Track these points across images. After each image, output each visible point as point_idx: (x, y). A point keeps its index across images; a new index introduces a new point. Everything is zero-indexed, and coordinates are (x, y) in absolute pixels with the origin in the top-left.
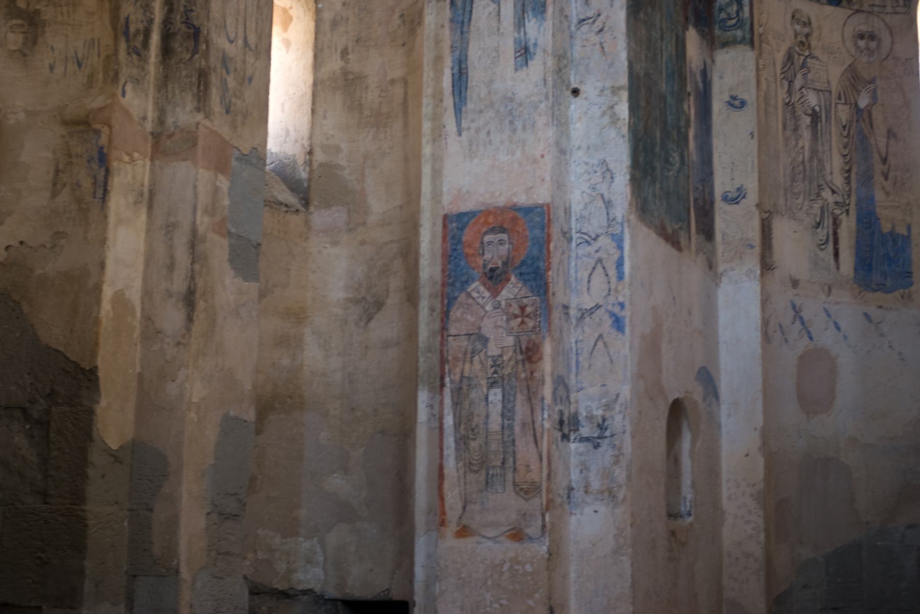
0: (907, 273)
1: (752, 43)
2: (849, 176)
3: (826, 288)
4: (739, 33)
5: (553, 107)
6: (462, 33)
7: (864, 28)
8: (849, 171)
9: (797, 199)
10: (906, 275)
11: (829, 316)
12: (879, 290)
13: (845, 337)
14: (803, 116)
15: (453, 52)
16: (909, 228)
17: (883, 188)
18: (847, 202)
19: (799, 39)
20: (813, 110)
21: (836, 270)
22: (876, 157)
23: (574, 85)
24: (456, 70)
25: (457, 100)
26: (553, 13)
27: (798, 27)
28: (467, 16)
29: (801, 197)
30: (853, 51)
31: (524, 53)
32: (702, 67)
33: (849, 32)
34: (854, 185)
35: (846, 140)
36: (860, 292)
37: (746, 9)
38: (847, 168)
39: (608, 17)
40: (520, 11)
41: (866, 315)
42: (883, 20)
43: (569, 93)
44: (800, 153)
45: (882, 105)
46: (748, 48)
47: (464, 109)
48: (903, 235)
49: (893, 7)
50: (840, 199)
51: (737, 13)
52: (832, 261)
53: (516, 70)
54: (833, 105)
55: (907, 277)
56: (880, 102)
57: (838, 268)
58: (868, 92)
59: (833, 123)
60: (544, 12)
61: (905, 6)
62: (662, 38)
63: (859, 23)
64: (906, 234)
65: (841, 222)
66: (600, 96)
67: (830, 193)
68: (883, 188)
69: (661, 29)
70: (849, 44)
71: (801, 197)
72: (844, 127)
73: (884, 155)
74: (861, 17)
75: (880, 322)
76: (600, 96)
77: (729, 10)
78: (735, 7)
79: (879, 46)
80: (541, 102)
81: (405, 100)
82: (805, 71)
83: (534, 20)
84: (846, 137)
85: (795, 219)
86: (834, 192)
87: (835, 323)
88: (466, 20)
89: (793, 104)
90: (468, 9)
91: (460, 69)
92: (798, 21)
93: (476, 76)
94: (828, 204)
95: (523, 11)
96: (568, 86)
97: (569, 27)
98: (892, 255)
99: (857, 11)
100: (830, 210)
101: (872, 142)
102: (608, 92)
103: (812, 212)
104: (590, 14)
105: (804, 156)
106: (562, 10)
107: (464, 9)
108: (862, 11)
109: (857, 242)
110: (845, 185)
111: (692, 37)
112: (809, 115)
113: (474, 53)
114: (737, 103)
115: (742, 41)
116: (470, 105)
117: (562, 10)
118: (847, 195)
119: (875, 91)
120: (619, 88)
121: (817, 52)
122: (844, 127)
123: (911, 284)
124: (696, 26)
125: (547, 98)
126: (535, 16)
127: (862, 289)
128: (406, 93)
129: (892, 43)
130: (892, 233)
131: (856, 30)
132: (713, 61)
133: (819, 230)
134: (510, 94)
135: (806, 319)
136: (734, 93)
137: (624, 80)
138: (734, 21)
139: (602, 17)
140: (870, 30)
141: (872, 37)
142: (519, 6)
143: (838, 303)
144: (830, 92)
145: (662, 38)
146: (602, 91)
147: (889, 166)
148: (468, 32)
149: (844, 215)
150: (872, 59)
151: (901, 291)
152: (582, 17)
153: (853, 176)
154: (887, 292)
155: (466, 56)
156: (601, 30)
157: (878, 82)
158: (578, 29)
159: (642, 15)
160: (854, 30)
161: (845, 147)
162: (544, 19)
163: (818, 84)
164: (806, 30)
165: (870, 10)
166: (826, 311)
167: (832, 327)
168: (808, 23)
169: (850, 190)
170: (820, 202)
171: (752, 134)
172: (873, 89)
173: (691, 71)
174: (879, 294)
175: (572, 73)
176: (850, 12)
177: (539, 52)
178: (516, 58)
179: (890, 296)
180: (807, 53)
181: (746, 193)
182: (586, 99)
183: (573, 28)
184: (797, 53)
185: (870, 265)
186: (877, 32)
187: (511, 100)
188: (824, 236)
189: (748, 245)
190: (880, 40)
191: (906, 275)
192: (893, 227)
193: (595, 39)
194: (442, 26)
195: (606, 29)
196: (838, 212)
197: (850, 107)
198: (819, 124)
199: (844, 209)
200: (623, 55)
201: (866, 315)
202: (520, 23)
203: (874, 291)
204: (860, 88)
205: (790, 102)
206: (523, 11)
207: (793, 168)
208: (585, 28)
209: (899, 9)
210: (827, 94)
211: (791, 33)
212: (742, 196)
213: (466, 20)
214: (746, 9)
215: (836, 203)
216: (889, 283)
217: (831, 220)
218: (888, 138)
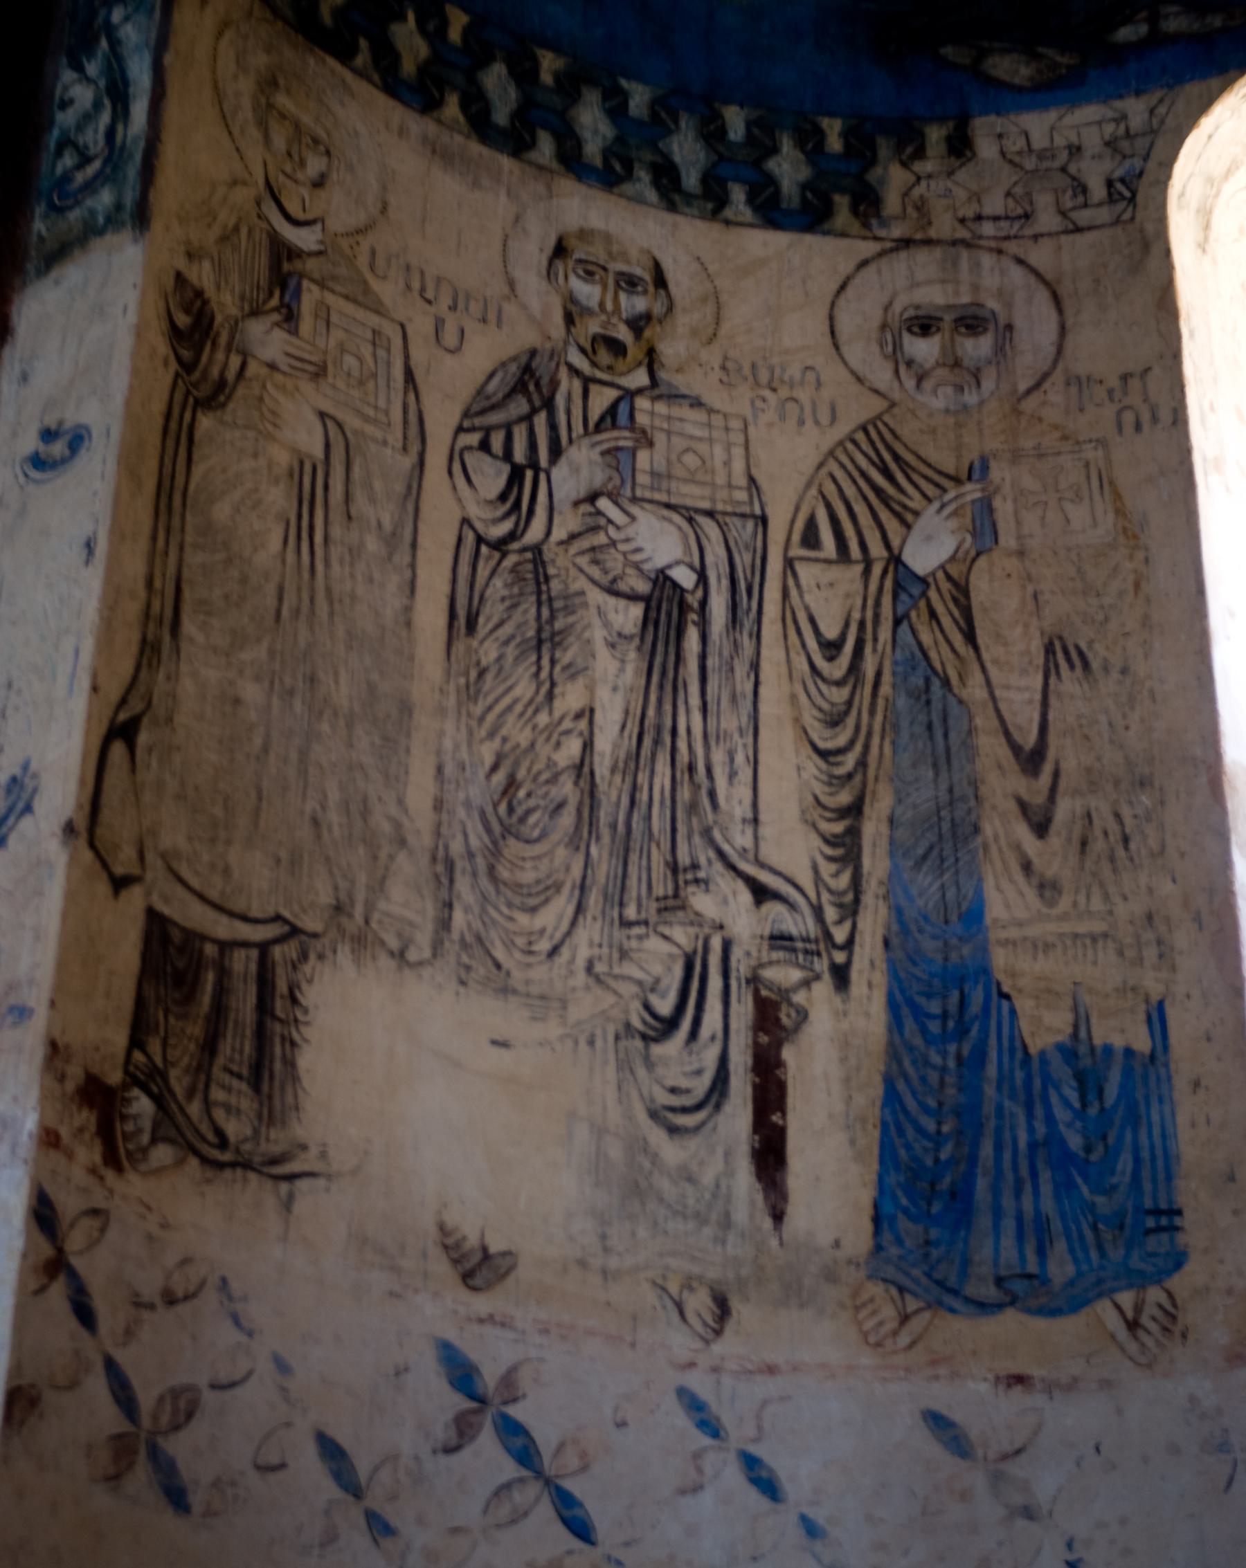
0: (1157, 1212)
2: (854, 833)
3: (700, 1302)
7: (934, 296)
8: (855, 810)
9: (533, 910)
10: (1150, 1222)
11: (710, 1427)
12: (1013, 1301)
13: (811, 1529)
14: (596, 596)
16: (1157, 1018)
17: (1027, 867)
18: (840, 935)
20: (662, 579)
21: (768, 1223)
22: (991, 747)
27: (588, 292)
29: (560, 908)
30: (882, 375)
34: (875, 863)
35: (839, 695)
36: (905, 1318)
37: (139, 110)
38: (844, 798)
41: (937, 1421)
42: (1020, 262)
44: (568, 732)
45: (1021, 553)
48: (1129, 1052)
49: (1063, 214)
50: (799, 924)
52: (744, 1179)
54: (775, 565)
55: (1159, 1229)
56: (1008, 540)
57: (778, 1217)
58: (955, 513)
59: (771, 629)
64: (1142, 1042)
65: (803, 1015)
67: (746, 896)
68: (1027, 867)
71: (560, 908)
72: (832, 648)
73: (1029, 740)
74: (925, 261)
75: (1018, 1452)
82: (625, 438)
84: (839, 683)
85: (506, 991)
86: (761, 894)
87: (750, 1463)
89: (537, 549)
92: (589, 272)
94: (727, 946)
98: (1075, 1142)
99: (906, 243)
100: (740, 965)
101: (975, 691)
103: (629, 969)
105: (588, 746)
108: (928, 242)
109: (891, 1097)
110: (827, 869)
112: (632, 597)
114: (58, 448)
118: (840, 906)
119: (986, 507)
122: (832, 648)
123: (1178, 1261)
127: (912, 1304)
129: (1063, 330)
130: (1069, 1053)
131: (897, 307)
133: (673, 1046)
135: (545, 1436)
136: (51, 422)
140: (965, 299)
143: (771, 1370)
144: (763, 520)
147: (1056, 774)
149: (823, 989)
150: (971, 398)
151: (1126, 1299)
153: (873, 829)
154: (1053, 1312)
157: (998, 472)
160: (886, 309)
161: (834, 721)
163: (686, 489)
164: (640, 304)
165: (962, 233)
166: (693, 1405)
167: (734, 1476)
169: (856, 884)
170: (682, 935)
171: (89, 546)
172: (981, 500)
174: (1011, 1319)
176: (870, 248)
179: (1069, 1327)
181: (35, 790)
184: (574, 371)
185: (961, 1197)
186: (992, 304)
188: (699, 1072)
189: (12, 1009)
191: (1150, 1222)
192: (1081, 1020)
196: (785, 974)
197: (867, 572)
198: (692, 638)
199: (822, 965)
201: (937, 1421)
203: (983, 1307)
204: (916, 502)
205: (512, 536)
207: (512, 784)
209: (1083, 217)
210: (744, 531)
212: (21, 805)
215: (779, 939)
216: (1060, 1268)
217: (743, 1011)
218: (1049, 671)
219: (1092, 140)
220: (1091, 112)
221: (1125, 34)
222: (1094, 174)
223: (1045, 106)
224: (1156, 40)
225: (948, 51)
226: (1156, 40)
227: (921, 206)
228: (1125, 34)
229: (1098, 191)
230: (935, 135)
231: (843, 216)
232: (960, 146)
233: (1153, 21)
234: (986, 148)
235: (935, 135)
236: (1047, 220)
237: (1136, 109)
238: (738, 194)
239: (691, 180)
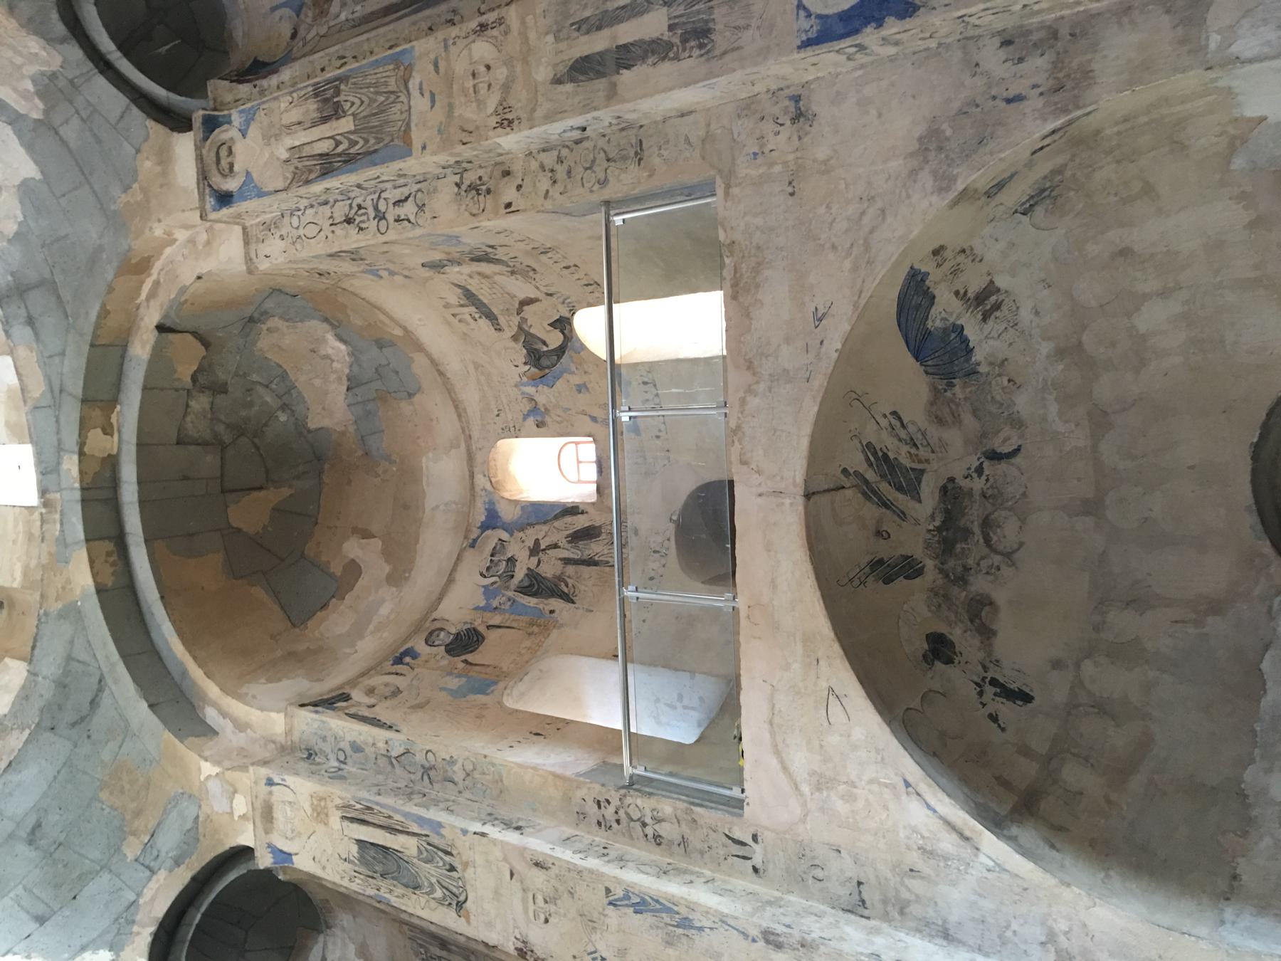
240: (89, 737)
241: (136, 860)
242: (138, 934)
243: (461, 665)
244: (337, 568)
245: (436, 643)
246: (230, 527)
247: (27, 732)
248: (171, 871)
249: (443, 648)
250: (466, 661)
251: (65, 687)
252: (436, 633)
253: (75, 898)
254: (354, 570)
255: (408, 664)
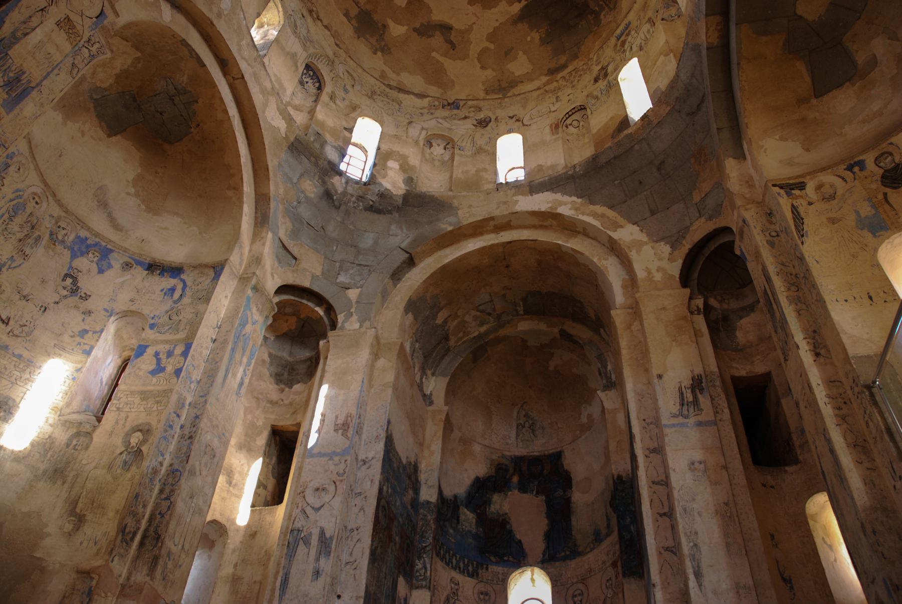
1: (429, 588)
4: (424, 583)
5: (326, 601)
6: (290, 561)
7: (483, 589)
15: (283, 569)
19: (453, 590)
23: (339, 593)
24: (284, 578)
25: (281, 593)
26: (334, 556)
27: (453, 585)
28: (294, 553)
30: (477, 599)
31: (317, 573)
32: (405, 596)
33: (476, 592)
37: (429, 572)
39: (359, 563)
40: (318, 554)
43: (336, 597)
46: (427, 590)
47: (283, 598)
51: (424, 574)
53: (312, 581)
60: (330, 555)
61: (502, 581)
62: (385, 578)
63: (482, 587)
66: (350, 600)
69: (386, 574)
70: (476, 596)
76: (350, 600)
77: (421, 572)
78: (424, 571)
79: (489, 599)
80: (320, 599)
81: (259, 591)
83: (324, 559)
88: (293, 555)
90: (295, 550)
91: (286, 578)
92: (453, 582)
93: (292, 582)
95: (320, 554)
96: (336, 593)
97: (341, 565)
99: (481, 581)
102: (354, 599)
104: (351, 560)
106: (338, 556)
107: (293, 550)
111: (401, 581)
113: (294, 571)
115: (425, 587)
116: (287, 596)
117: (338, 556)
120: (359, 597)
121: (461, 598)
124: (404, 576)
125: (324, 597)
126: (325, 557)
128: (260, 589)
129: (496, 598)
132: (411, 595)
134: (307, 593)
137: (362, 594)
138: (422, 577)
139: (357, 562)
141: (487, 594)
142: (318, 551)
145: (385, 578)
146: (351, 597)
148: (293, 561)
152: (347, 561)
155: (290, 572)
156: (355, 568)
158: (345, 567)
159: (376, 565)
162: (329, 559)
164: (456, 587)
168: (458, 584)
173: (399, 597)
175: (339, 587)
176: (477, 581)
177: (324, 575)
178: (312, 575)
180: (456, 598)
182: (343, 600)
183: (343, 566)
187: (307, 596)
190: (490, 596)
193: (352, 572)
194: (282, 557)
195: (358, 568)
200: (364, 581)
202: (317, 559)
206: (320, 554)
208: (348, 567)
209: (499, 583)
211: (449, 588)
213: (293, 555)
214: (429, 572)
219: (501, 572)
220: (501, 568)
221: (506, 558)
222: (501, 577)
223: (496, 566)
224: (508, 560)
225: (487, 555)
226: (508, 560)
227: (482, 576)
228: (506, 558)
229: (501, 580)
230: (485, 566)
231: (475, 577)
232: (487, 569)
233: (508, 557)
234: (490, 570)
235: (485, 566)
236: (495, 582)
237: (506, 569)
238: (466, 572)
239: (462, 569)
240: (693, 125)
241: (696, 204)
242: (684, 246)
243: (881, 196)
244: (861, 59)
245: (882, 164)
246: (796, 14)
247: (669, 108)
248: (707, 221)
249: (882, 171)
250: (885, 194)
251: (688, 91)
252: (886, 155)
253: (668, 209)
254: (873, 62)
255: (854, 173)
